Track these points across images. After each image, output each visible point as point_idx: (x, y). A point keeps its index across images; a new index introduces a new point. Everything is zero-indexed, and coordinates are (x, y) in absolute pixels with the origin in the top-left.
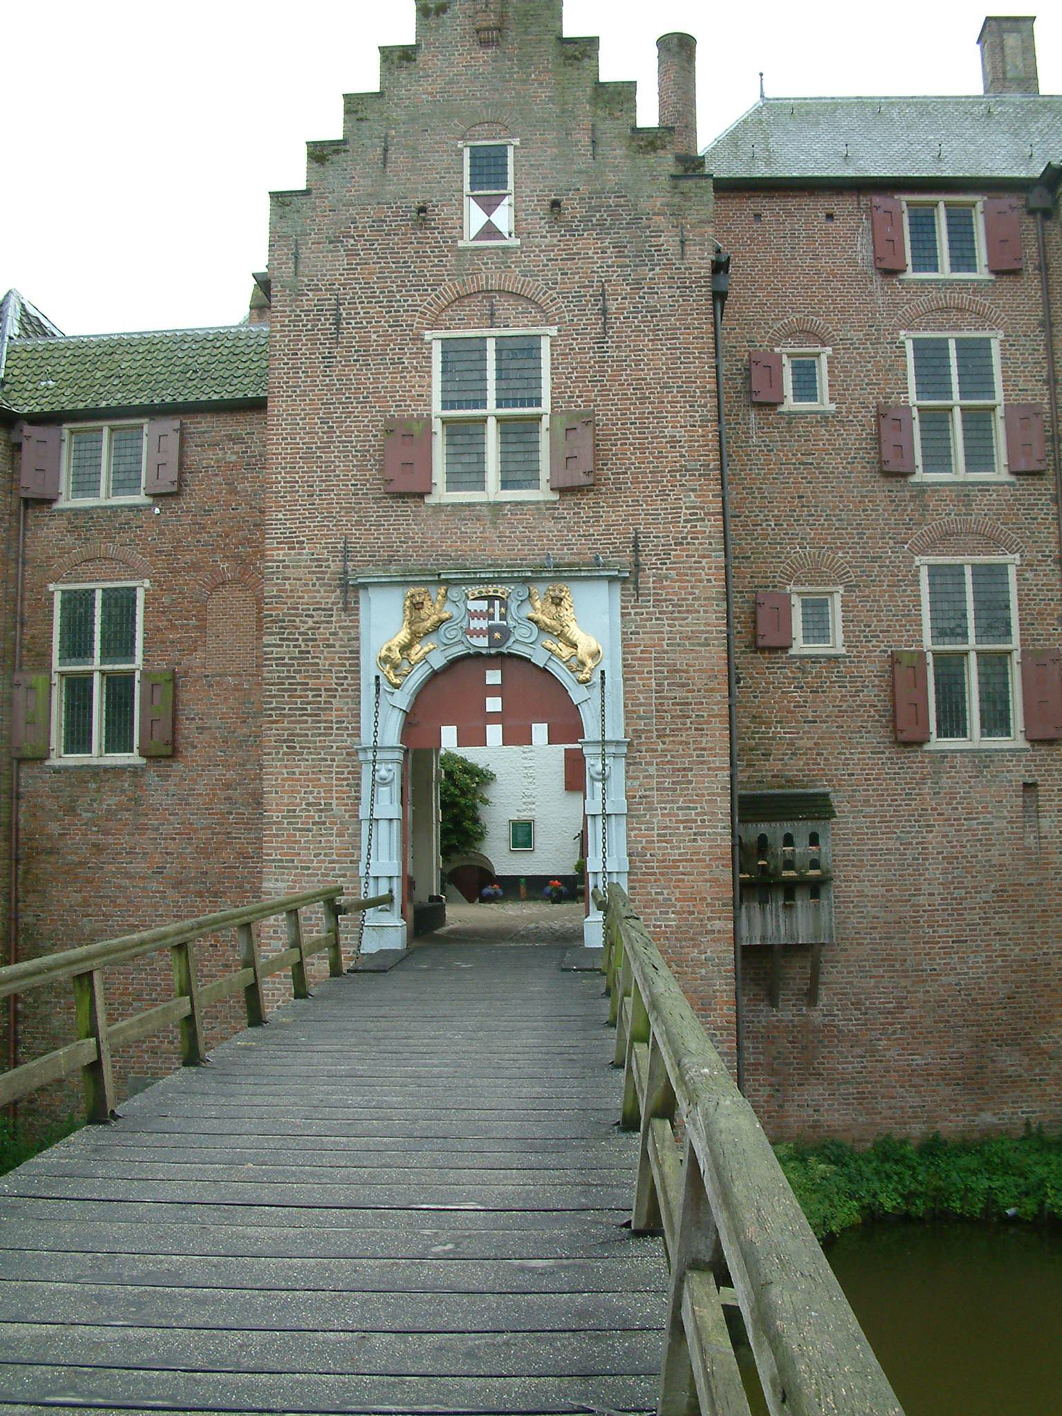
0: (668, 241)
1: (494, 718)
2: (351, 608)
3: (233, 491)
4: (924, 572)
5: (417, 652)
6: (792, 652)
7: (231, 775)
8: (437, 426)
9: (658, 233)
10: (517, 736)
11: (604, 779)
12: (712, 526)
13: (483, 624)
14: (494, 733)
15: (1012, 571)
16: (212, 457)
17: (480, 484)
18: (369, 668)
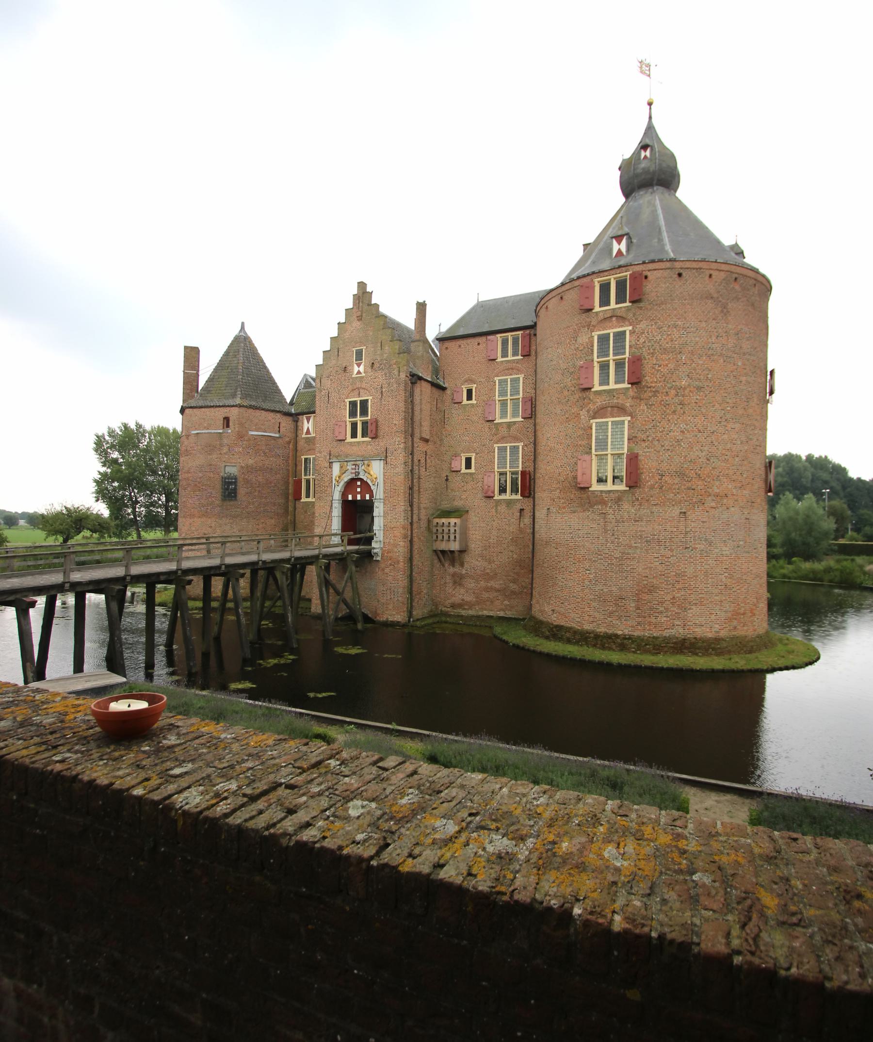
4: (496, 449)
15: (521, 448)
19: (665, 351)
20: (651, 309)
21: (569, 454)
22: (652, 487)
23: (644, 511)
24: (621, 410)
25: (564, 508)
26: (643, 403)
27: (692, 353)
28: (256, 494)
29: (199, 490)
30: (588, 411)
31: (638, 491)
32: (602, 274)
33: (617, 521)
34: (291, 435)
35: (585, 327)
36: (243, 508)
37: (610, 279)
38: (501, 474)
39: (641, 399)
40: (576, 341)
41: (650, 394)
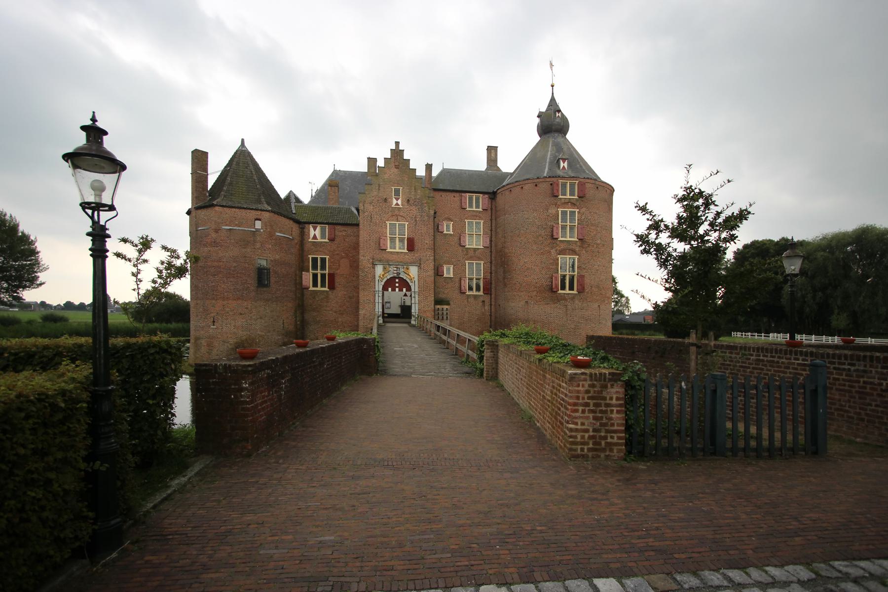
0: (426, 208)
1: (397, 287)
2: (374, 268)
3: (344, 240)
5: (385, 276)
6: (444, 276)
7: (345, 293)
8: (388, 238)
9: (425, 207)
10: (401, 290)
11: (415, 298)
12: (432, 258)
13: (396, 272)
14: (397, 289)
16: (340, 234)
17: (395, 248)
18: (377, 278)
19: (592, 225)
20: (587, 202)
21: (544, 272)
22: (588, 293)
23: (585, 305)
24: (574, 252)
25: (541, 302)
26: (584, 250)
27: (601, 227)
28: (282, 282)
29: (234, 277)
30: (556, 250)
31: (582, 294)
32: (563, 179)
33: (573, 309)
34: (297, 239)
35: (553, 204)
36: (273, 294)
37: (567, 182)
38: (470, 279)
39: (583, 248)
40: (547, 211)
41: (587, 246)
